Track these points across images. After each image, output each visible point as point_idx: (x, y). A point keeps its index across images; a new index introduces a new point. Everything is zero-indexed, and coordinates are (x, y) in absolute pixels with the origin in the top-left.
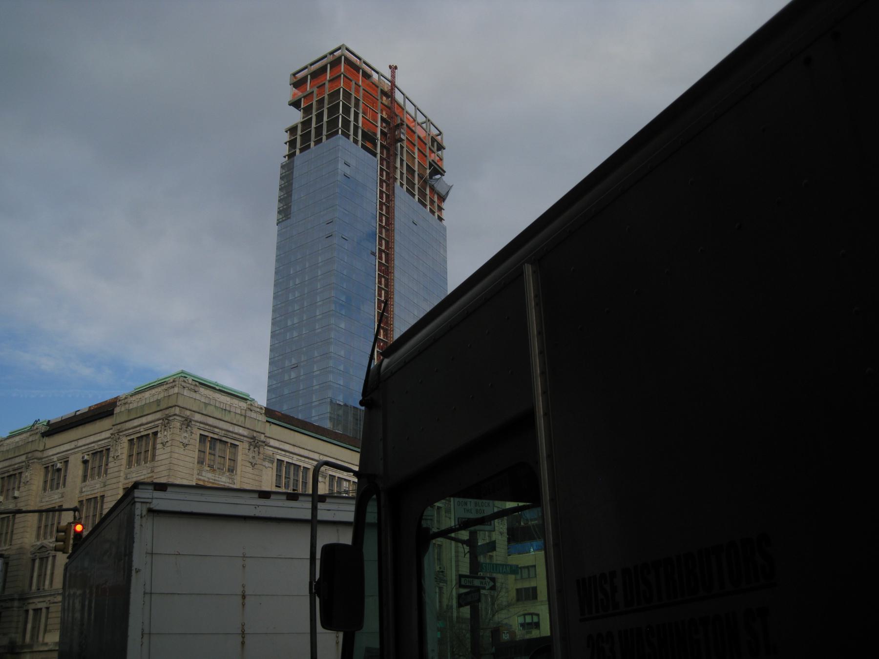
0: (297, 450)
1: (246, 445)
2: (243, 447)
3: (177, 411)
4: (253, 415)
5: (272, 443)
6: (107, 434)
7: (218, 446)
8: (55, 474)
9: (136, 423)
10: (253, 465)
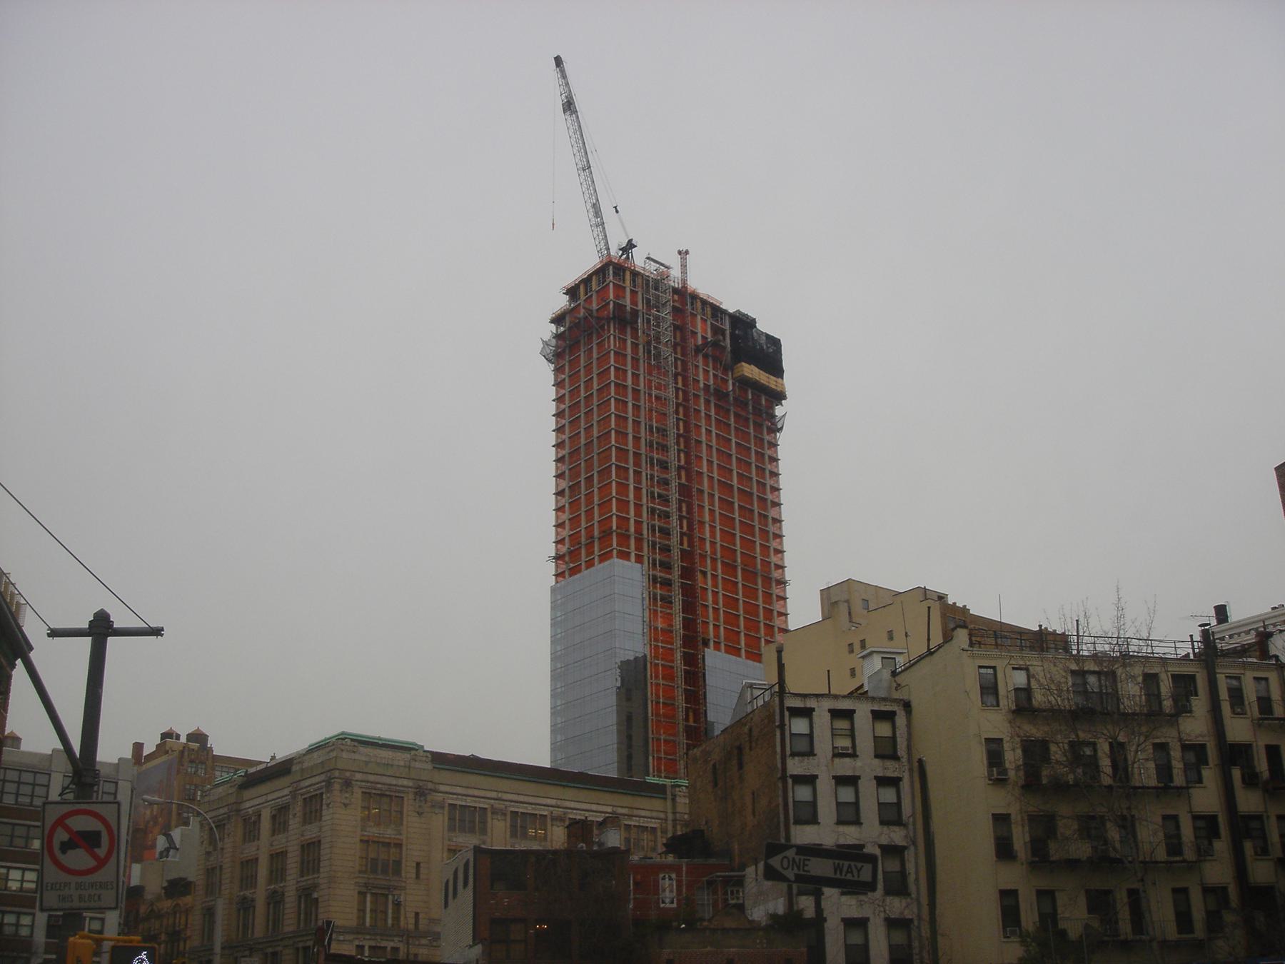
0: (471, 792)
1: (411, 796)
2: (409, 799)
3: (337, 774)
4: (417, 765)
5: (442, 788)
6: (286, 791)
7: (386, 800)
8: (251, 827)
9: (307, 783)
10: (420, 814)
